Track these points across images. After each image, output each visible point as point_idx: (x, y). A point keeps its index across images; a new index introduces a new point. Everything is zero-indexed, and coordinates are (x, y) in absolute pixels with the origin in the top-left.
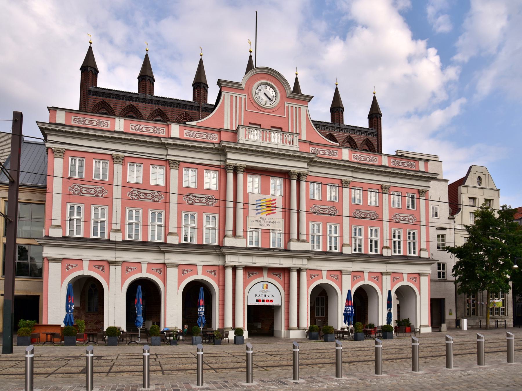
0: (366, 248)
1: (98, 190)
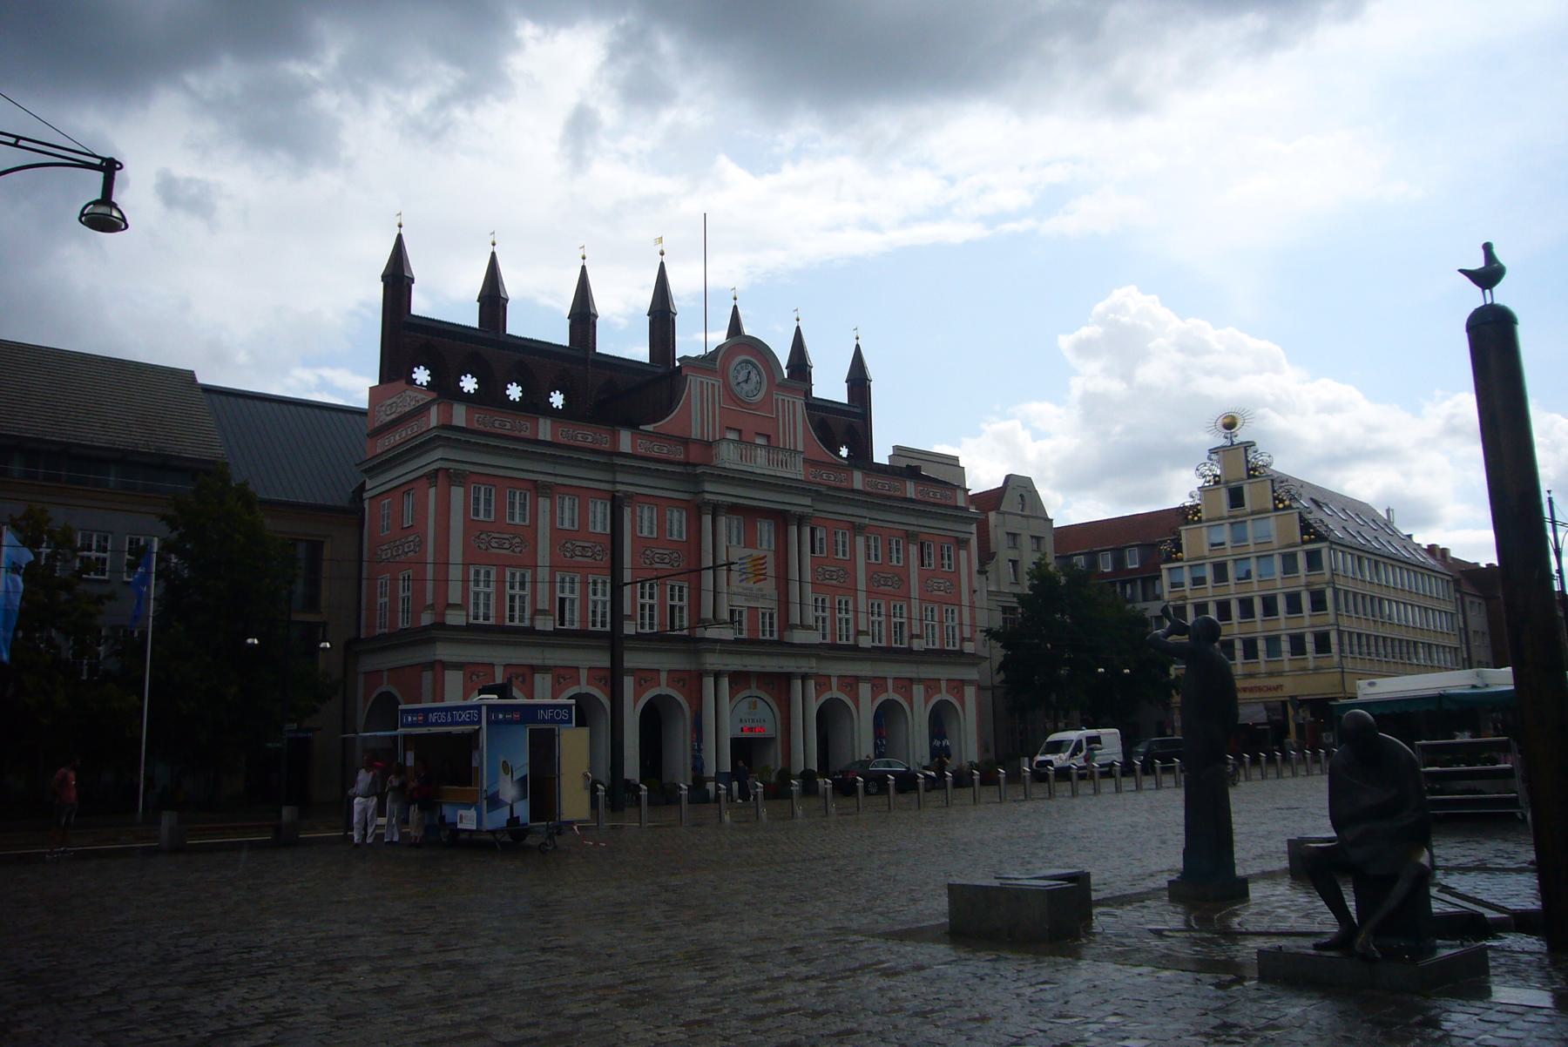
0: (889, 637)
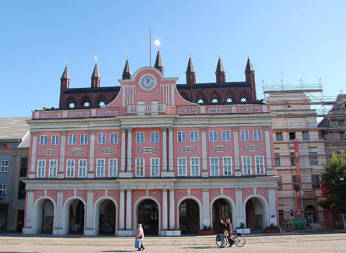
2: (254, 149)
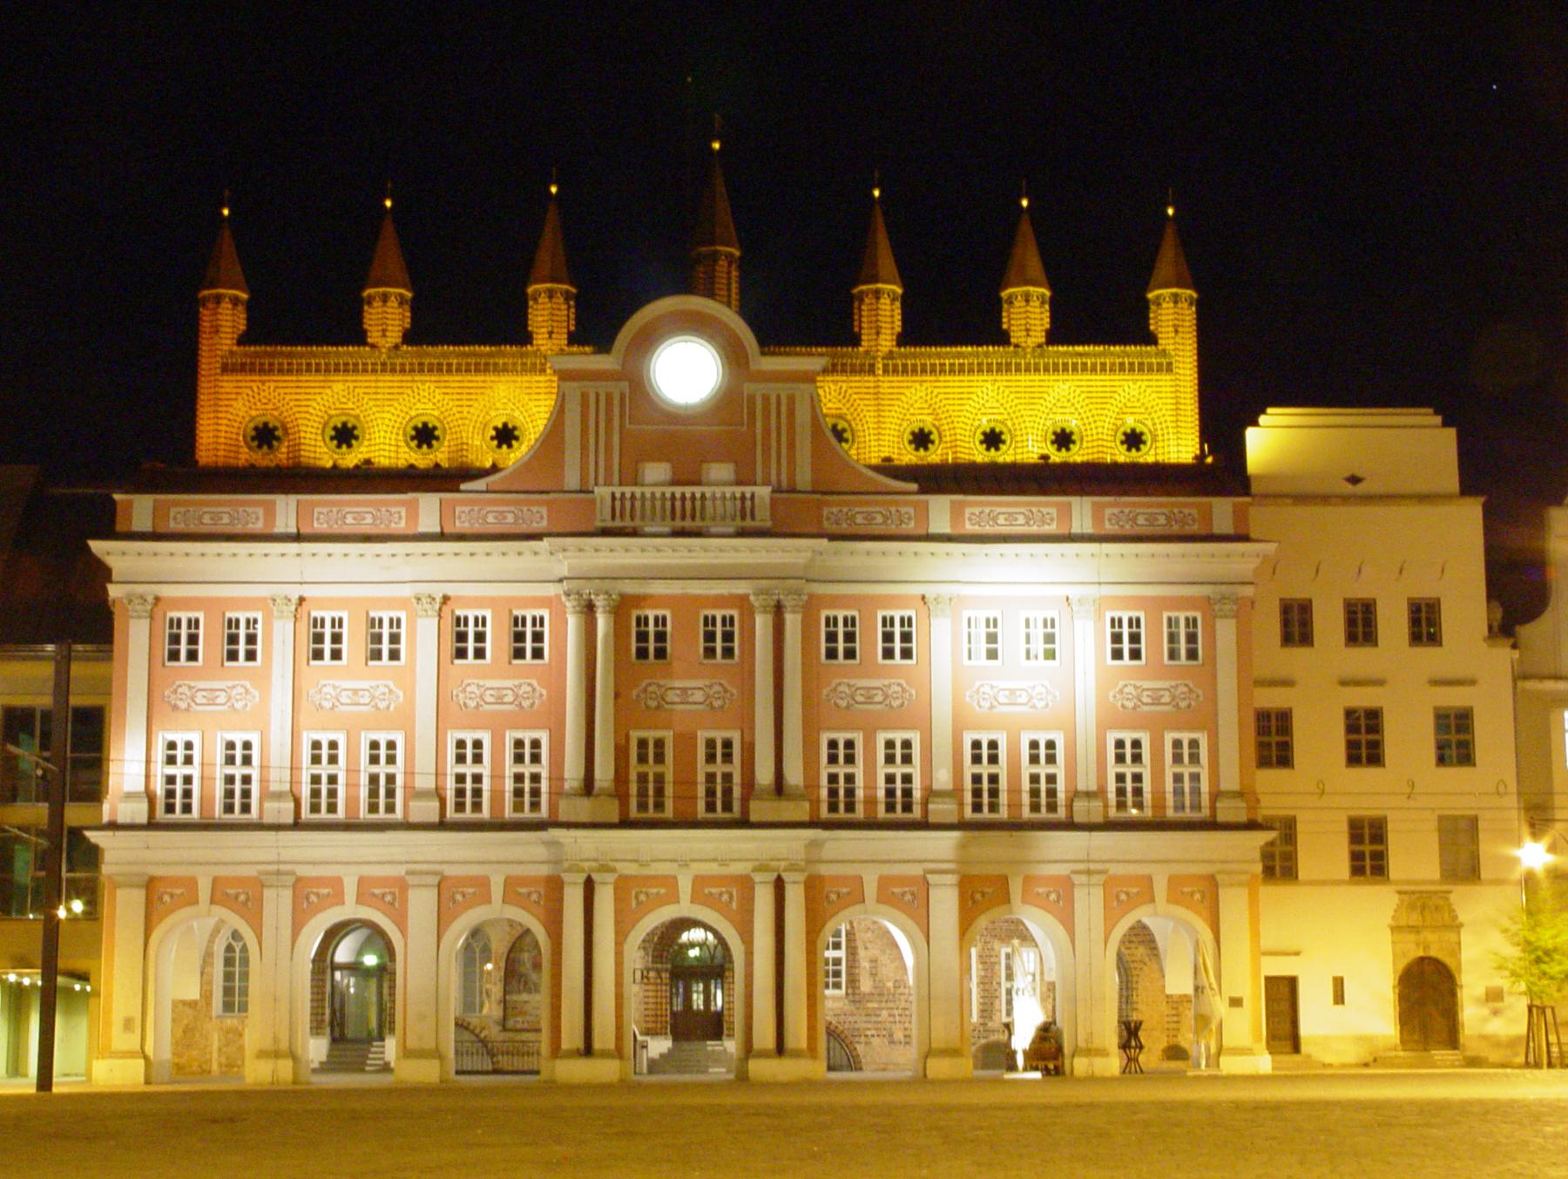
1: (234, 692)
2: (1163, 700)
